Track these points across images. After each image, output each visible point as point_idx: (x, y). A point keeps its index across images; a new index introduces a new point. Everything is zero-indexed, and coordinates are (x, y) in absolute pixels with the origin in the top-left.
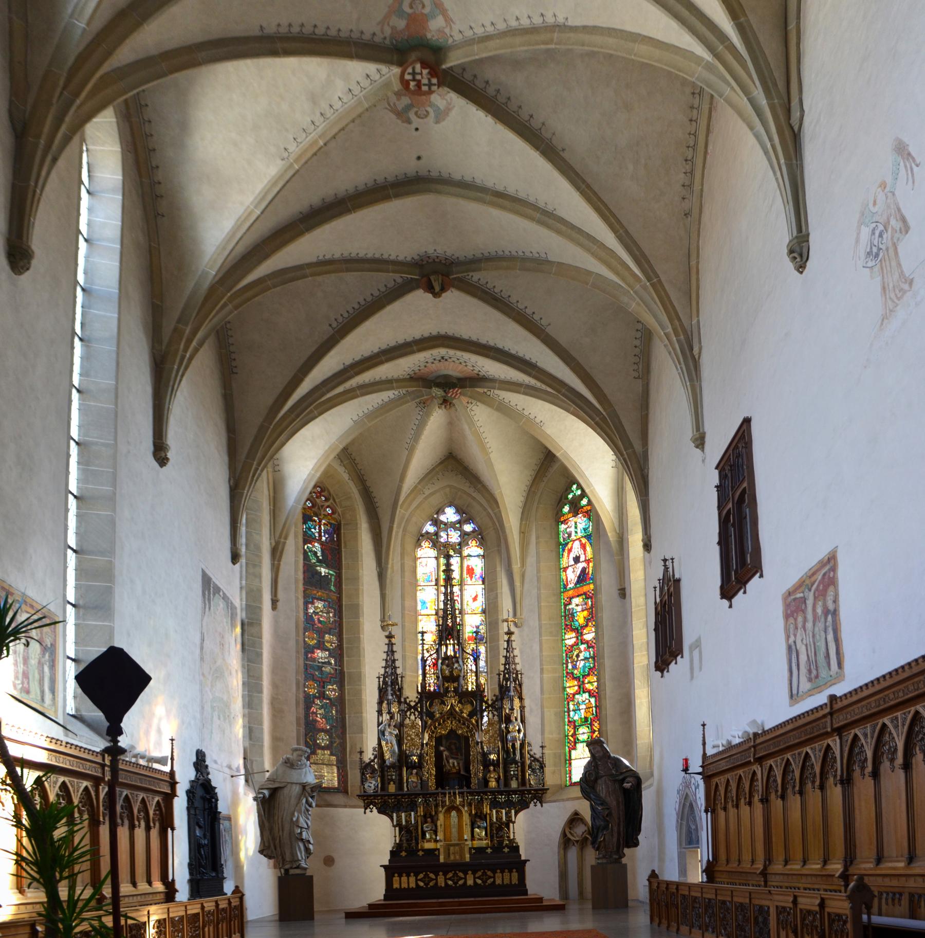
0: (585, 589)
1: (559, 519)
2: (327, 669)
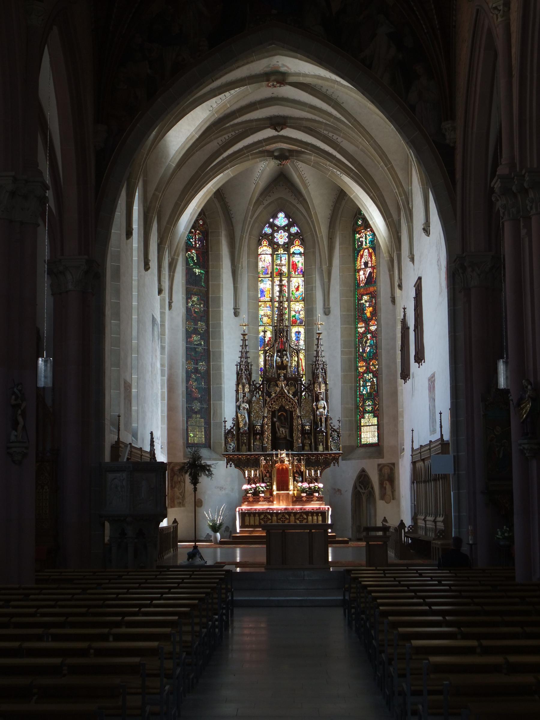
0: (372, 289)
1: (356, 230)
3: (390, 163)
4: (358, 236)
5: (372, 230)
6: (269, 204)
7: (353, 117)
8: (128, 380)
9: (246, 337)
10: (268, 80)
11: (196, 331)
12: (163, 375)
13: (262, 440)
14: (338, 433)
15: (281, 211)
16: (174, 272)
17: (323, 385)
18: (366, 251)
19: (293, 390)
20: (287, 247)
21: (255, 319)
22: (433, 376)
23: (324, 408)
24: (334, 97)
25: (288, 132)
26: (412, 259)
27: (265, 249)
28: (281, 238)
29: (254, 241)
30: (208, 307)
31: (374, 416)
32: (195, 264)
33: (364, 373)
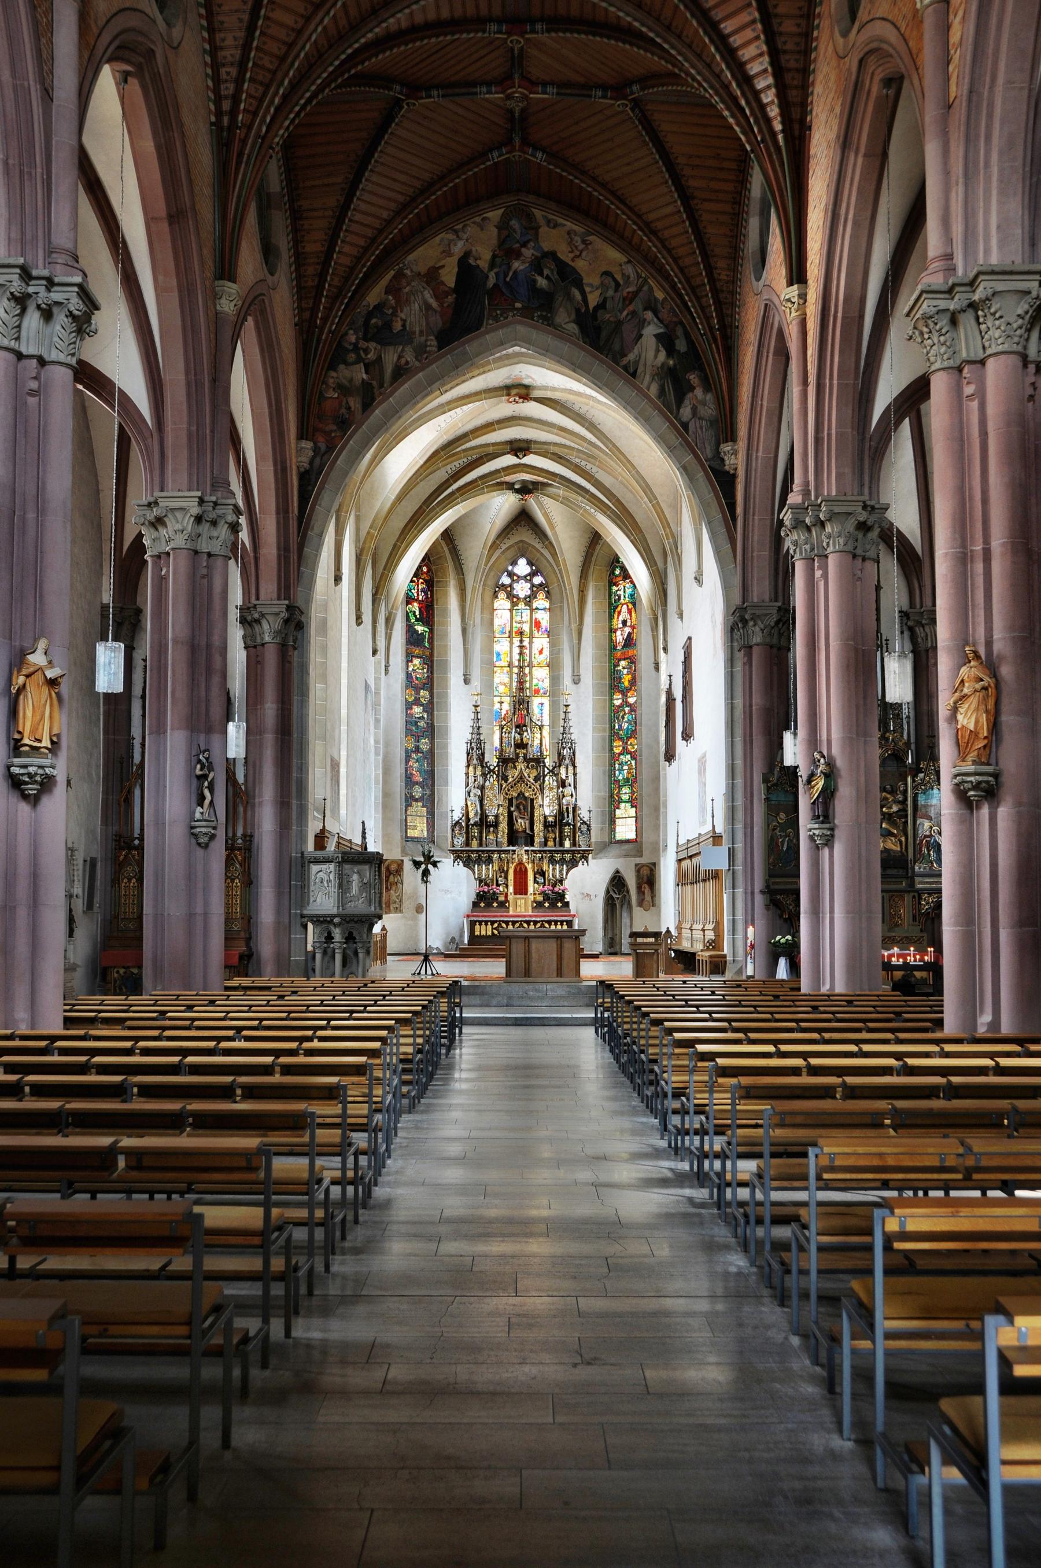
0: (630, 654)
1: (612, 582)
2: (422, 724)
3: (656, 498)
4: (614, 588)
5: (632, 582)
6: (508, 549)
7: (611, 442)
8: (336, 757)
9: (479, 709)
10: (508, 395)
11: (417, 702)
12: (377, 754)
13: (496, 832)
14: (589, 826)
15: (522, 556)
16: (391, 630)
17: (571, 768)
18: (625, 606)
19: (534, 773)
20: (529, 600)
21: (489, 686)
22: (704, 756)
23: (572, 795)
24: (588, 416)
25: (531, 459)
26: (681, 616)
27: (502, 603)
28: (522, 589)
29: (489, 593)
30: (432, 673)
31: (632, 806)
32: (417, 620)
33: (620, 754)
